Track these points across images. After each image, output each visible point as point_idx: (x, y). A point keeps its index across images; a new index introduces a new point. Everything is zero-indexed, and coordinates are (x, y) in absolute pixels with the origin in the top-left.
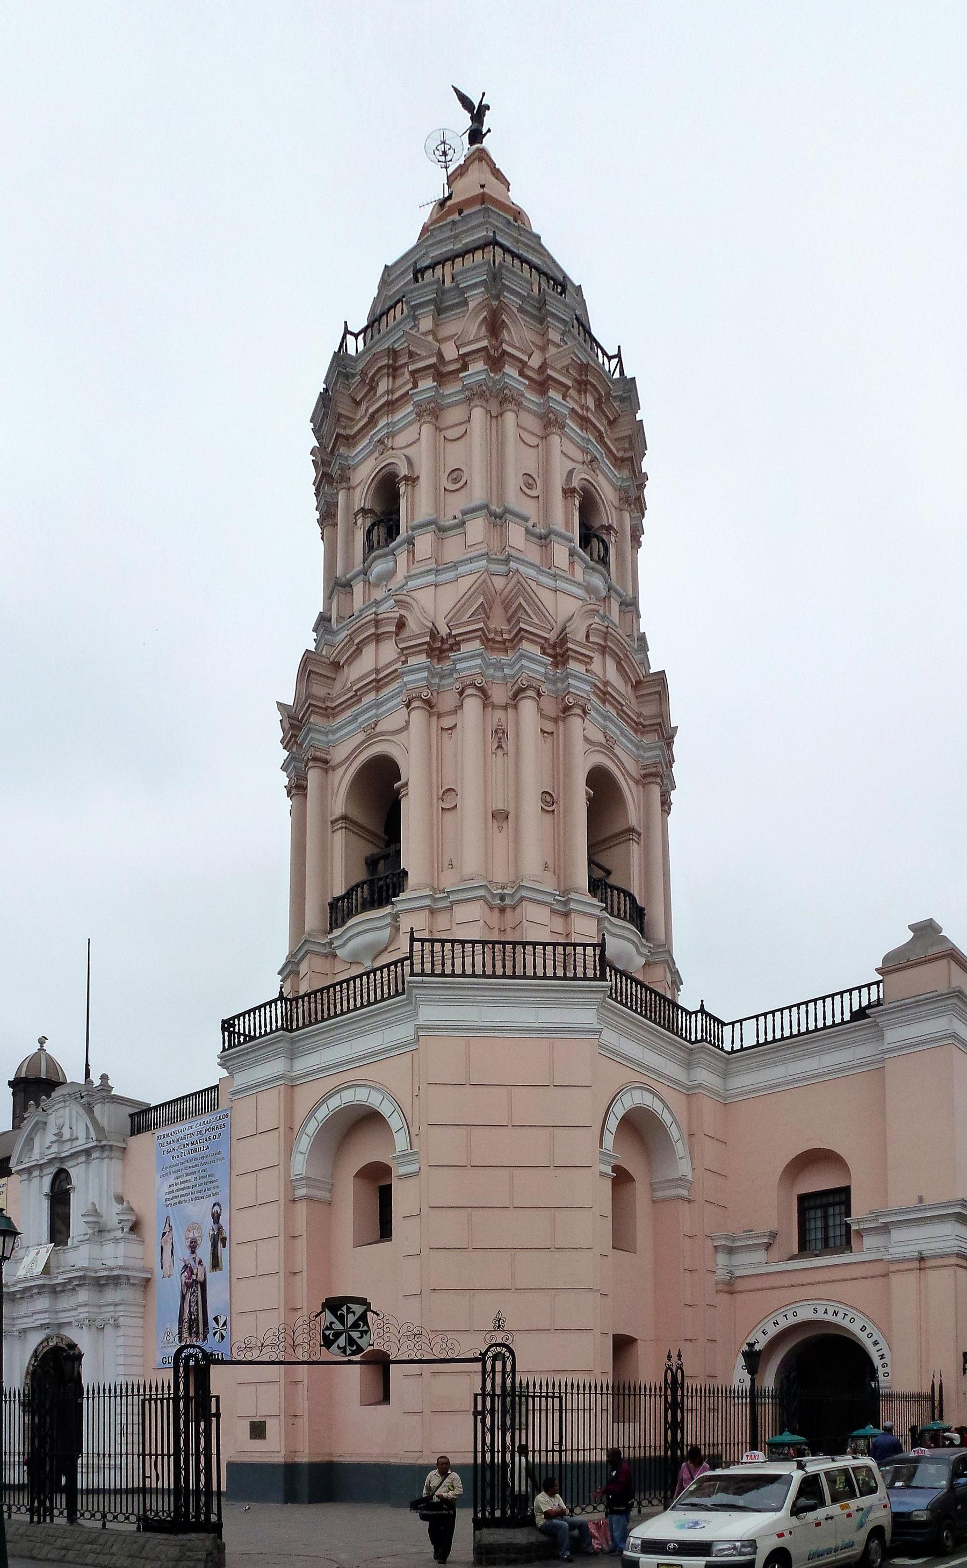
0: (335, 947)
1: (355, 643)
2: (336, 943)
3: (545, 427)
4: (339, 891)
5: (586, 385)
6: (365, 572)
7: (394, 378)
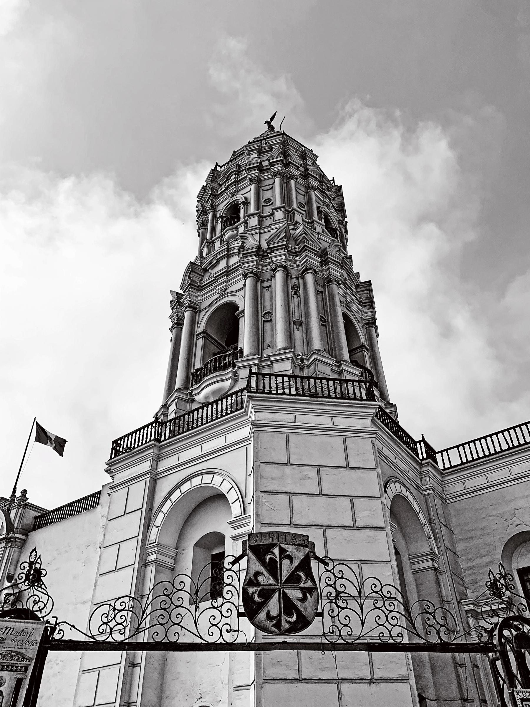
0: (194, 394)
1: (216, 259)
2: (194, 392)
3: (307, 189)
4: (198, 365)
5: (322, 183)
6: (221, 236)
7: (238, 175)
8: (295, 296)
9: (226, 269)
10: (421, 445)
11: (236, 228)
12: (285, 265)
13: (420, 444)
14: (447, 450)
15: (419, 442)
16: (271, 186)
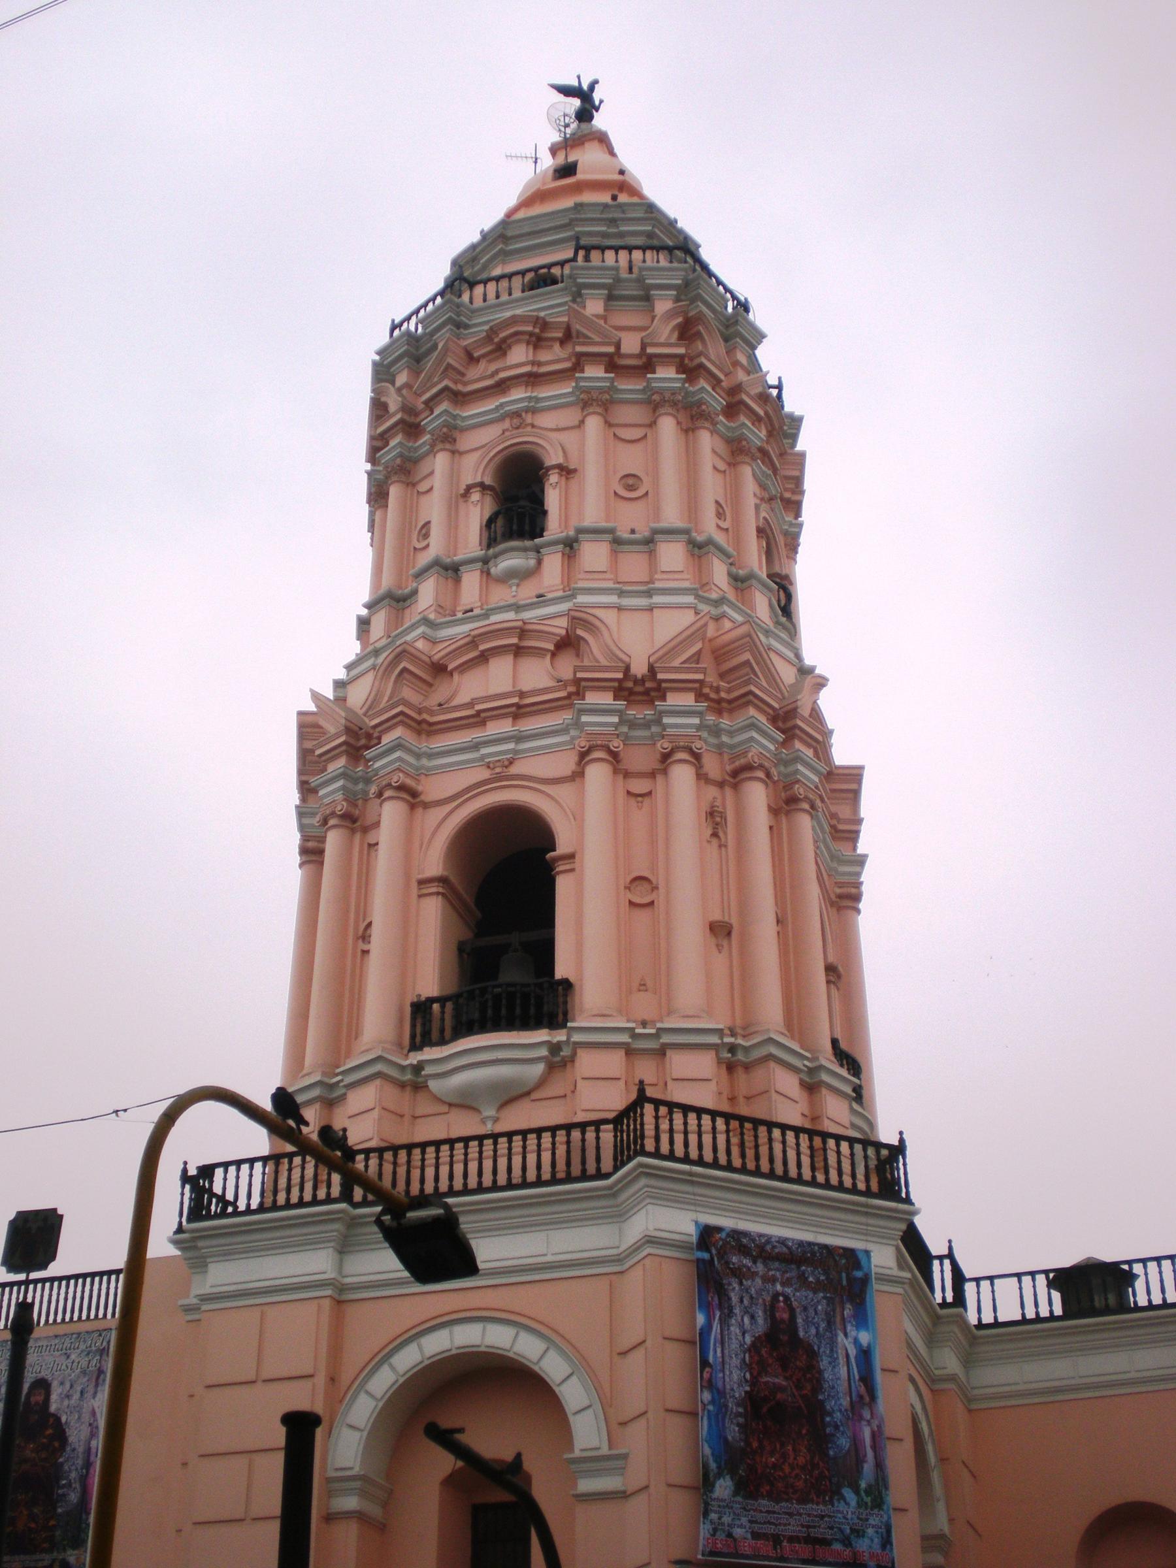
2: (428, 1070)
8: (715, 841)
9: (515, 700)
10: (945, 1268)
11: (537, 550)
12: (698, 747)
13: (941, 1264)
14: (991, 1279)
15: (940, 1258)
16: (637, 433)
